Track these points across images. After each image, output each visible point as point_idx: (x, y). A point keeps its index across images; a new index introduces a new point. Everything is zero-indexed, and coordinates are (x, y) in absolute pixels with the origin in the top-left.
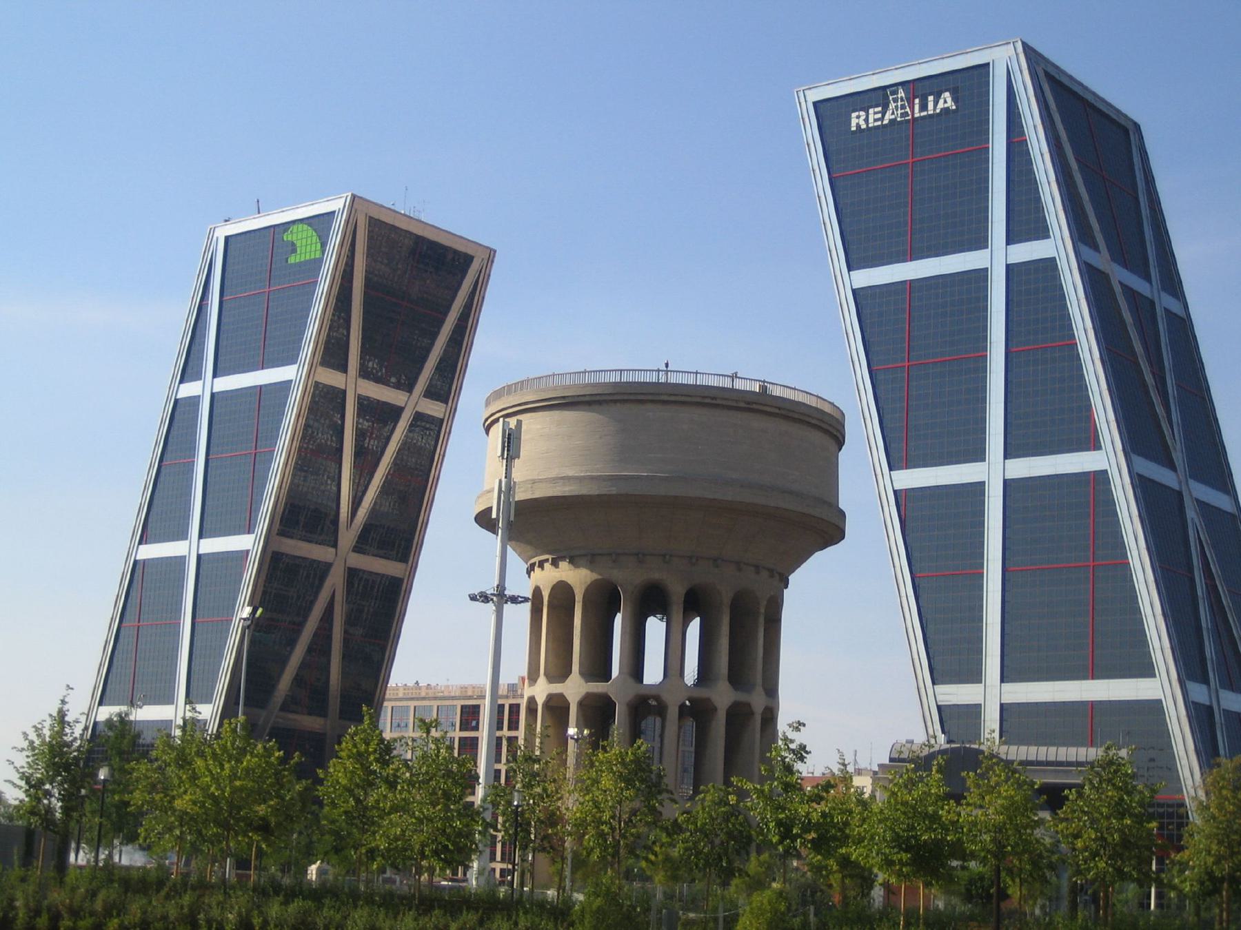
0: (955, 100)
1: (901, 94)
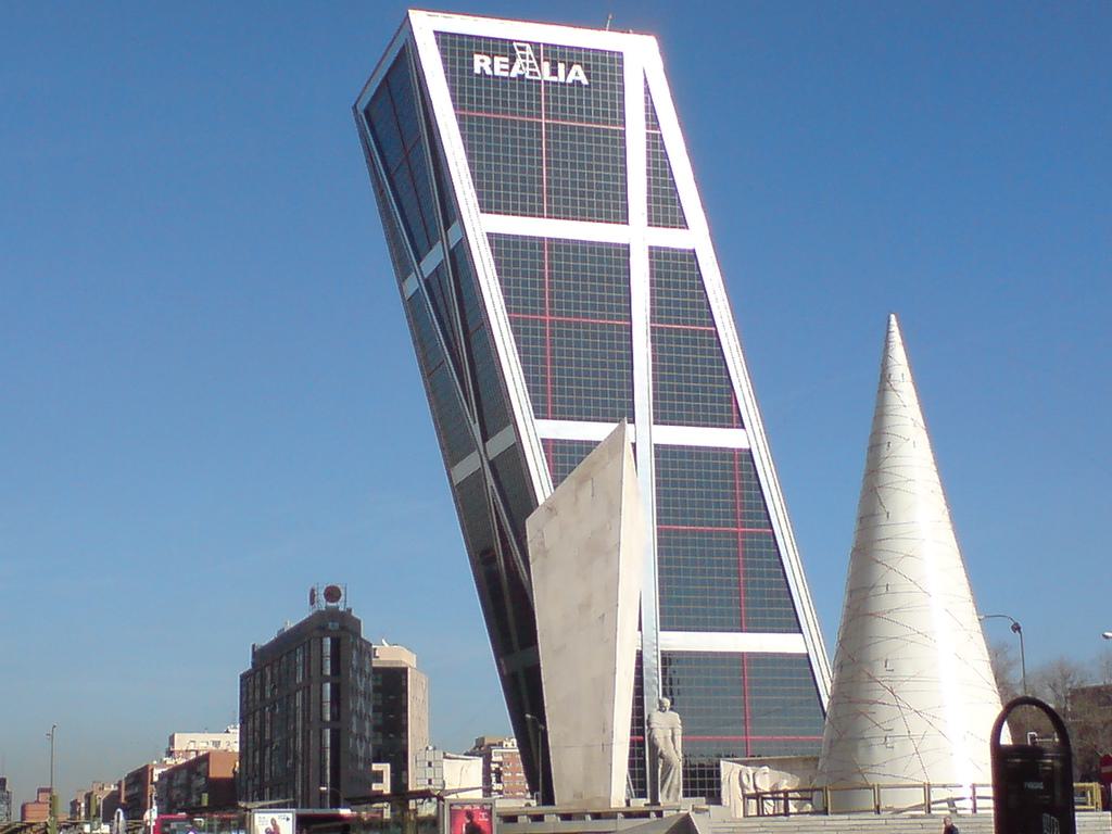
0: (588, 76)
1: (529, 52)
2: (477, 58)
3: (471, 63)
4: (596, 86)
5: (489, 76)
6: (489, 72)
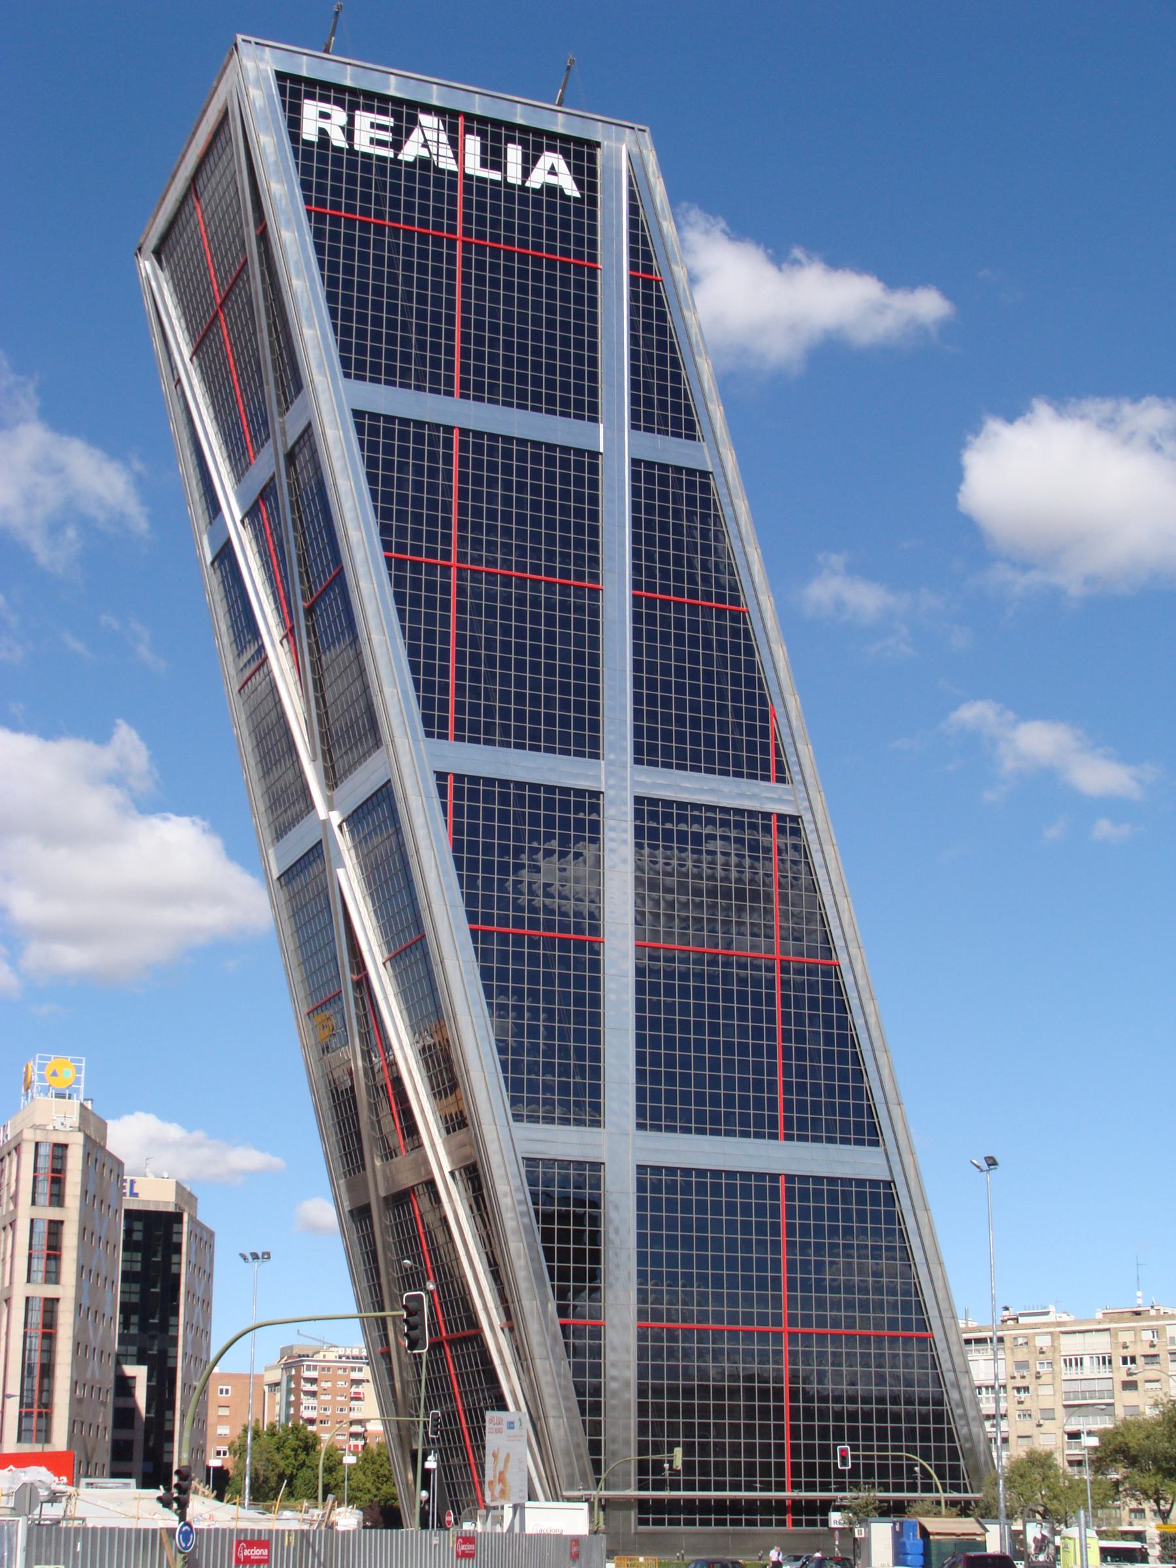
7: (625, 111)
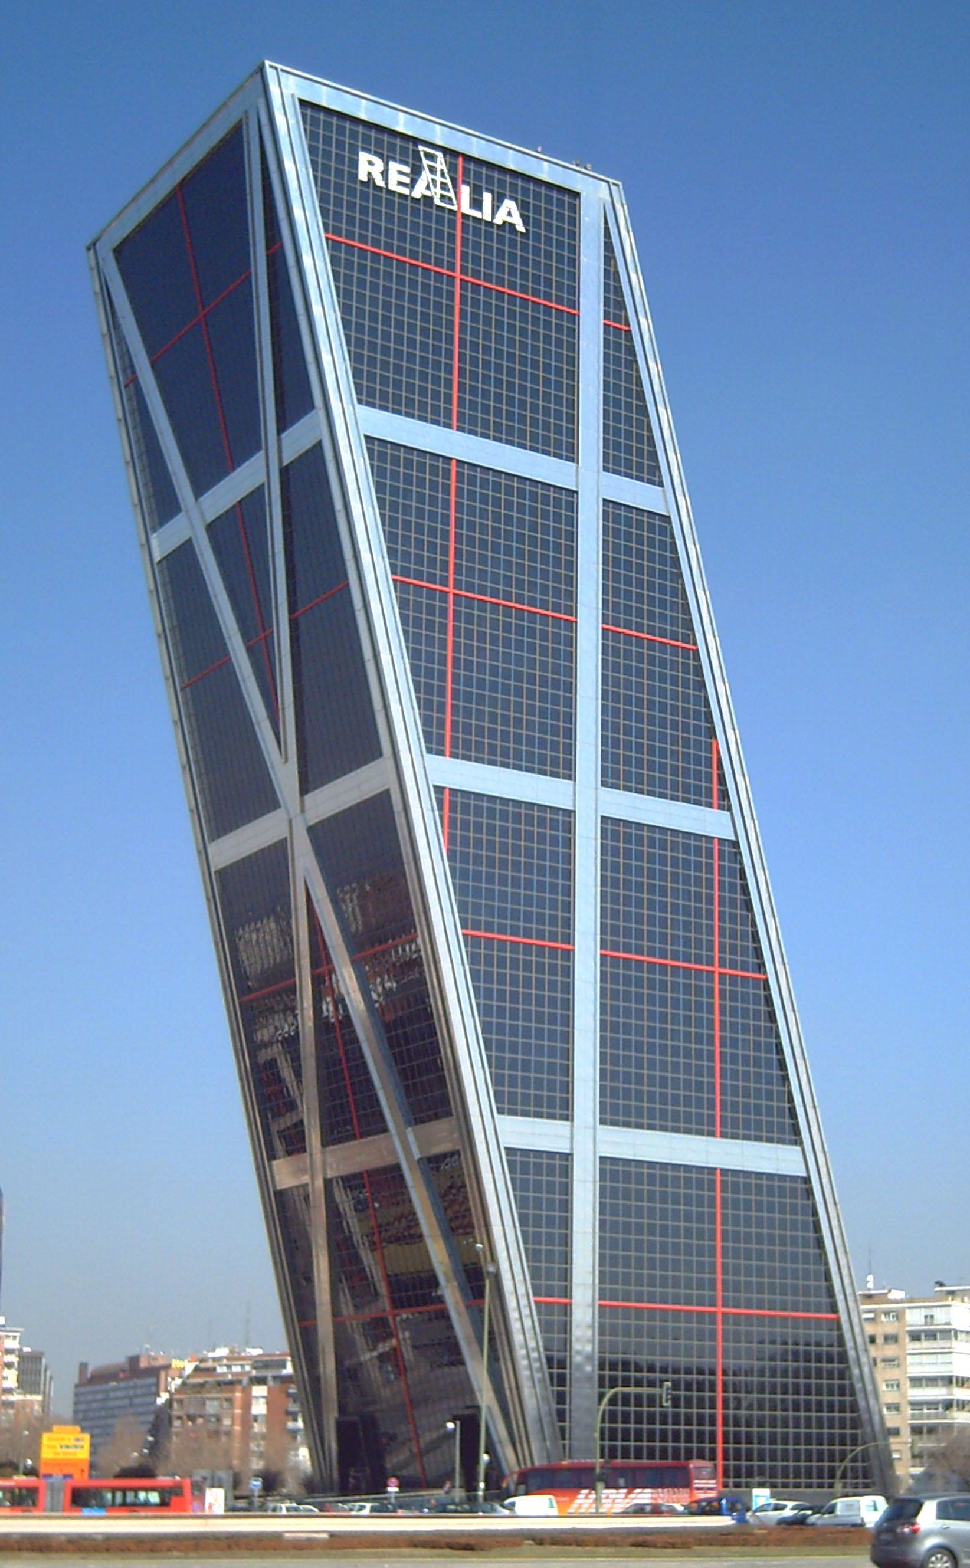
0: (525, 219)
1: (441, 164)
2: (364, 157)
3: (354, 164)
4: (537, 237)
5: (381, 188)
6: (380, 182)
7: (602, 165)
